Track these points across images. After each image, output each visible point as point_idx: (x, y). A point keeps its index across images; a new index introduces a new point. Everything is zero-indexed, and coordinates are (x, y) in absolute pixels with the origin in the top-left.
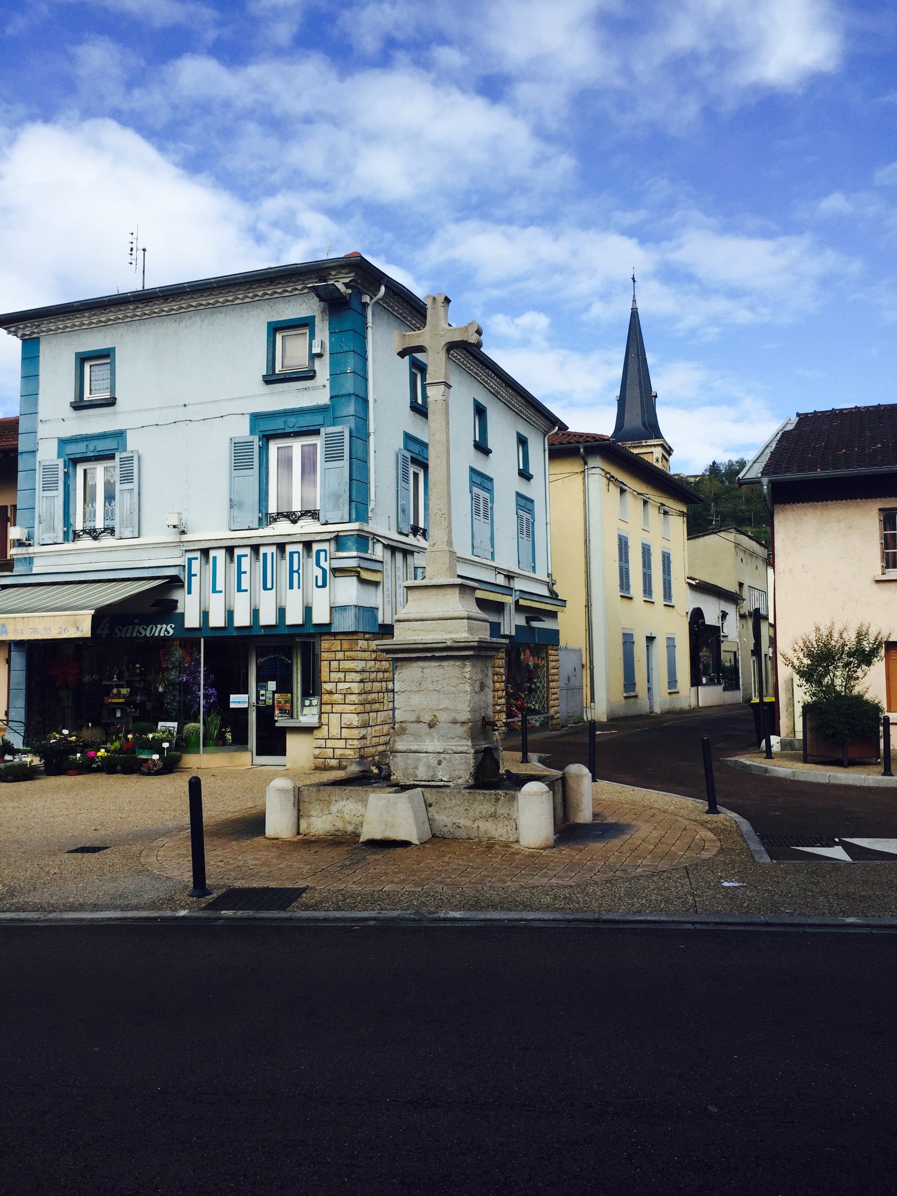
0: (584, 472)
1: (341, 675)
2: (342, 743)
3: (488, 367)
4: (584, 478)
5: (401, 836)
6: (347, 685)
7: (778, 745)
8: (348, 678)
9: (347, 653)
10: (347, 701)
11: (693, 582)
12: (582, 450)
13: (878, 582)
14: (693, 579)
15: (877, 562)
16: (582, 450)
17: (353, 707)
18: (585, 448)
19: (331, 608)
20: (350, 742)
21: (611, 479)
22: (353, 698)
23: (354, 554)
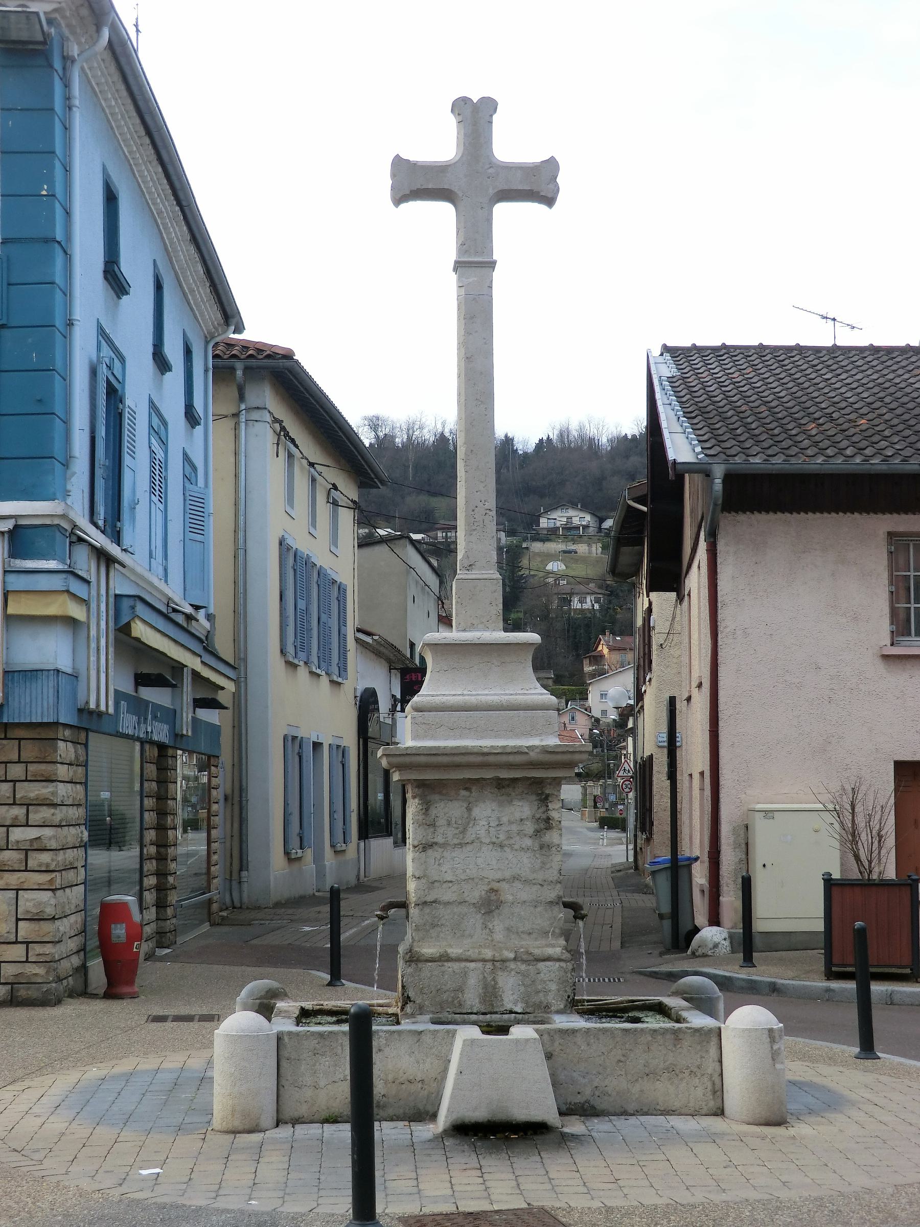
0: (236, 415)
1: (18, 812)
2: (18, 952)
3: (179, 203)
4: (236, 428)
5: (521, 1113)
6: (32, 833)
7: (727, 943)
8: (34, 817)
9: (32, 768)
10: (32, 864)
11: (368, 639)
12: (239, 373)
13: (886, 657)
14: (369, 634)
15: (884, 627)
16: (239, 373)
17: (46, 877)
18: (246, 369)
19: (6, 672)
20: (37, 949)
21: (283, 434)
22: (45, 857)
23: (52, 565)
